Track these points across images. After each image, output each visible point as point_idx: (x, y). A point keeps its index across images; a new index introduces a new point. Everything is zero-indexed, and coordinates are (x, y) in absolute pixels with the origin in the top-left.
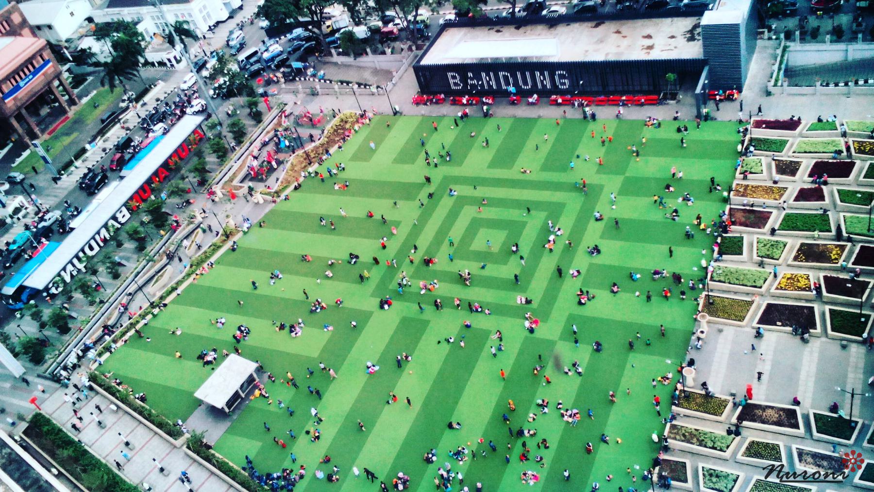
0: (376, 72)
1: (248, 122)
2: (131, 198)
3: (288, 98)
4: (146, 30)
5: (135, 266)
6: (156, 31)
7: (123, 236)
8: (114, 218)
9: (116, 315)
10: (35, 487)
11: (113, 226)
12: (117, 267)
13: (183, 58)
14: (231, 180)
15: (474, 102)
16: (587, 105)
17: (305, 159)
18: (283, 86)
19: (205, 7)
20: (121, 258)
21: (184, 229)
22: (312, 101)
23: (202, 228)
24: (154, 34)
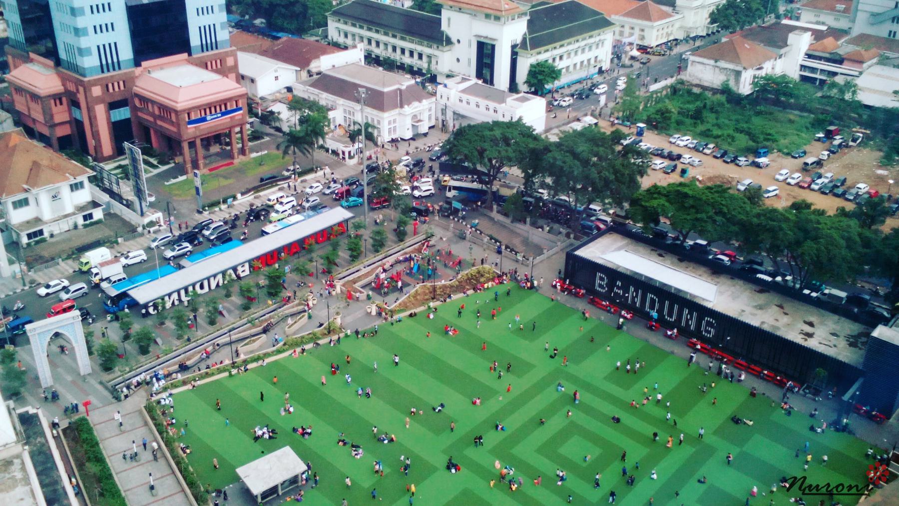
0: (526, 242)
1: (391, 236)
2: (259, 258)
3: (438, 232)
4: (334, 118)
5: (233, 320)
6: (343, 123)
7: (235, 289)
8: (235, 269)
9: (197, 358)
10: (51, 488)
11: (230, 275)
12: (217, 314)
13: (356, 157)
14: (354, 281)
15: (612, 310)
16: (726, 363)
17: (431, 293)
18: (437, 218)
19: (395, 121)
20: (224, 307)
21: (293, 307)
22: (457, 243)
23: (309, 314)
24: (340, 125)
